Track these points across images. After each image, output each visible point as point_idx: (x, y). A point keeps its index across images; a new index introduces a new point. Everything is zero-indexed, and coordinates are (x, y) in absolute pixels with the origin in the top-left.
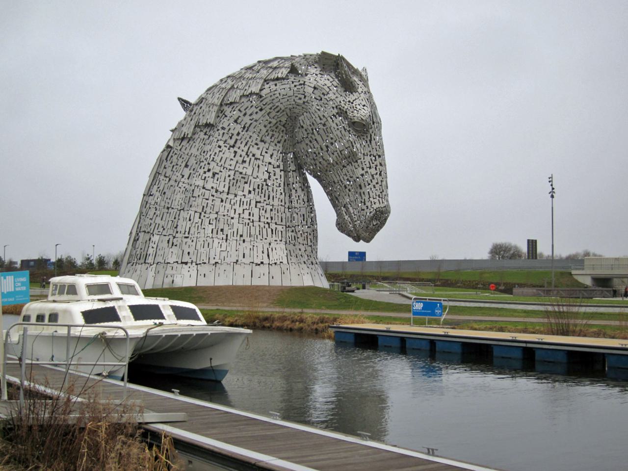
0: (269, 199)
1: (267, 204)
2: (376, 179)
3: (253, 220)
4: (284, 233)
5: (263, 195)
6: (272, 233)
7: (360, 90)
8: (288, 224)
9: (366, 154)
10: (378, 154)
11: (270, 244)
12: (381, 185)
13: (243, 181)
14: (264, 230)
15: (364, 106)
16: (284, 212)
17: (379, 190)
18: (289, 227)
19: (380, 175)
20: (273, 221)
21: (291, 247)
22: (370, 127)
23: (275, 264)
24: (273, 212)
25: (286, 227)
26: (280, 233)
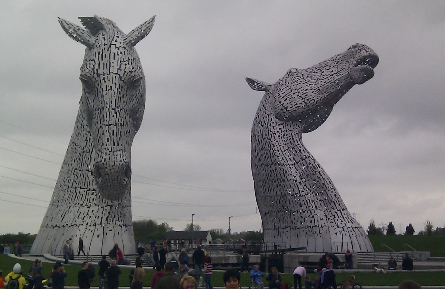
0: (81, 166)
1: (80, 170)
2: (99, 133)
3: (69, 186)
4: (84, 196)
5: (79, 162)
6: (75, 198)
7: (95, 46)
8: (89, 187)
9: (96, 109)
10: (103, 106)
11: (69, 208)
12: (102, 139)
13: (75, 151)
14: (72, 194)
15: (93, 60)
16: (88, 176)
17: (100, 144)
18: (90, 190)
19: (102, 128)
20: (79, 186)
21: (85, 209)
22: (94, 80)
23: (63, 226)
24: (82, 177)
25: (87, 190)
26: (81, 195)
